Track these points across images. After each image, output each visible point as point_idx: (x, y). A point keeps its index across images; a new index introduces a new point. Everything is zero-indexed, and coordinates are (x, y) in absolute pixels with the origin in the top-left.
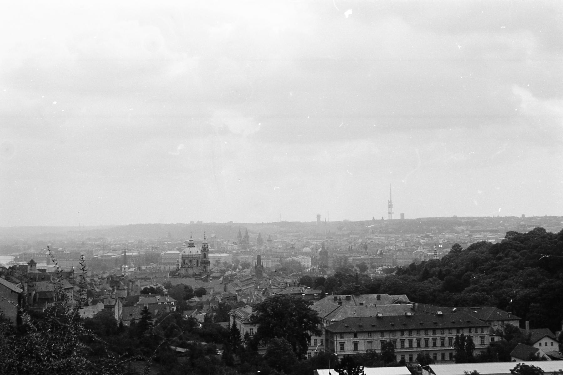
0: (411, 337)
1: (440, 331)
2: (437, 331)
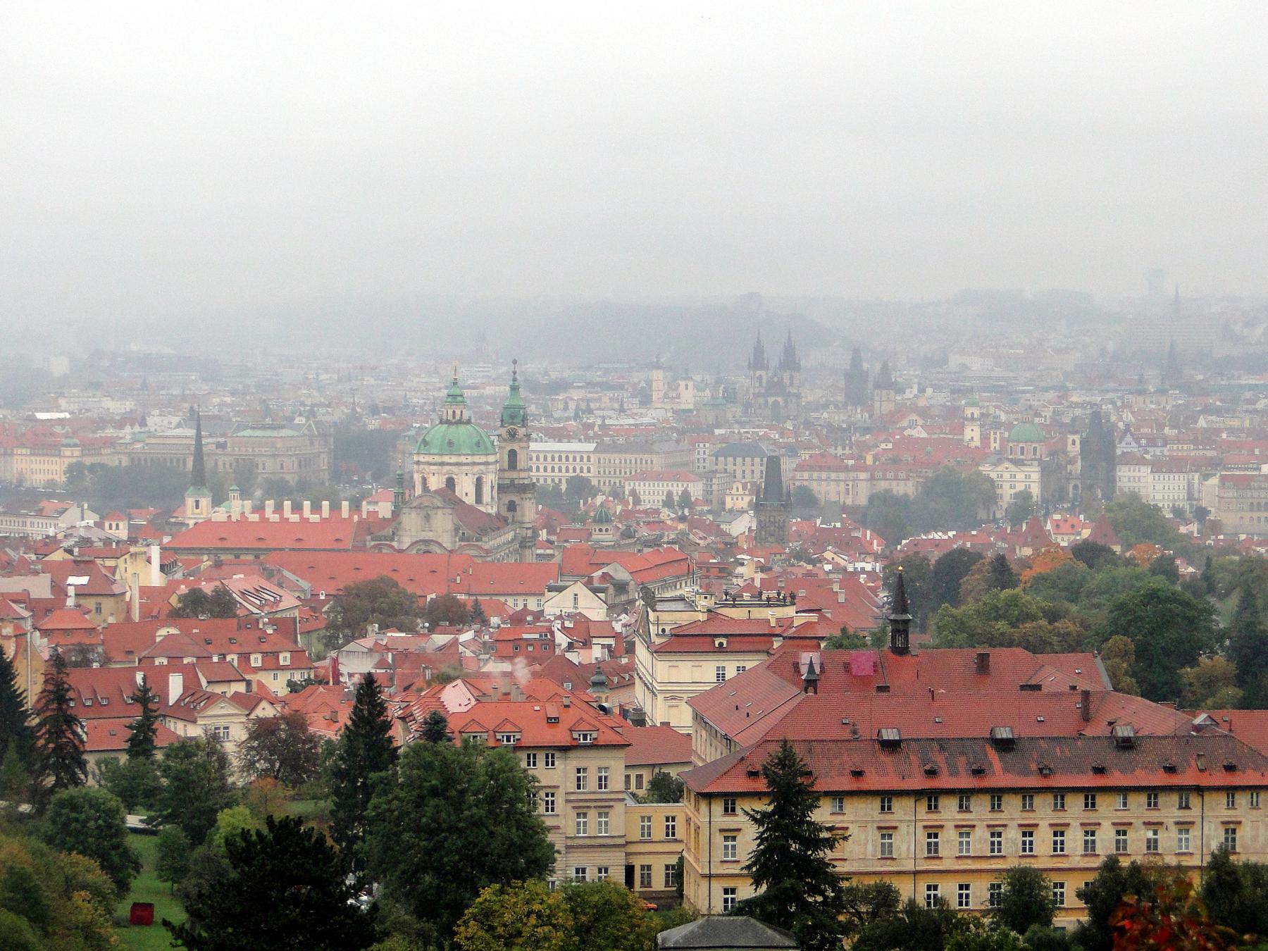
0: (998, 818)
1: (1175, 798)
2: (1038, 800)
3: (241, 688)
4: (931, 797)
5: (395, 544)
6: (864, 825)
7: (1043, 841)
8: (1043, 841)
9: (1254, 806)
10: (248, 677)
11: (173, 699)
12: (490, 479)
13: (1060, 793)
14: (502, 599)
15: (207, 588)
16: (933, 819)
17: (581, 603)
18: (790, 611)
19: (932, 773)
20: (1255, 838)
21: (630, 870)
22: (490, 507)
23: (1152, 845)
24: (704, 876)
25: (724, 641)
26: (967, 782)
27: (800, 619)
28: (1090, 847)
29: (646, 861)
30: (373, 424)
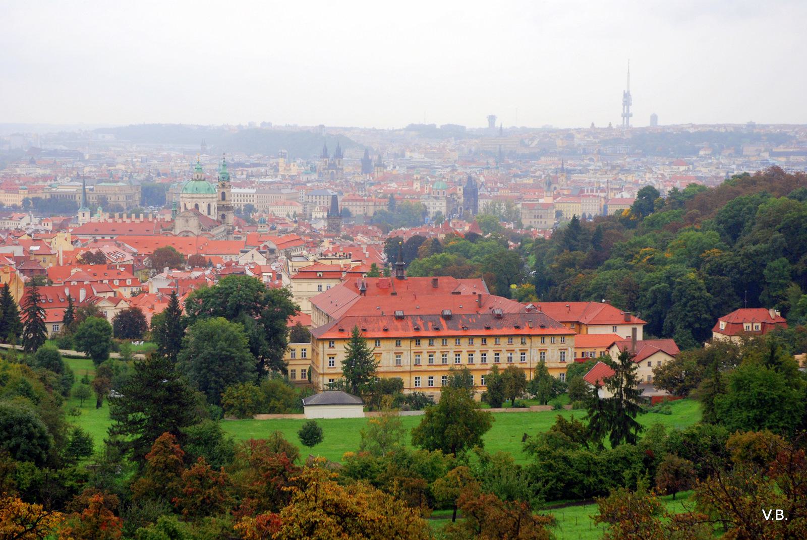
0: (445, 349)
3: (112, 294)
4: (417, 340)
5: (173, 232)
6: (388, 351)
7: (464, 359)
9: (553, 343)
10: (114, 290)
12: (214, 205)
13: (471, 338)
14: (221, 256)
15: (94, 252)
16: (418, 349)
17: (255, 258)
18: (349, 261)
19: (417, 329)
20: (553, 357)
22: (214, 216)
23: (510, 359)
24: (320, 374)
25: (321, 274)
26: (432, 333)
27: (354, 265)
28: (484, 360)
29: (293, 368)
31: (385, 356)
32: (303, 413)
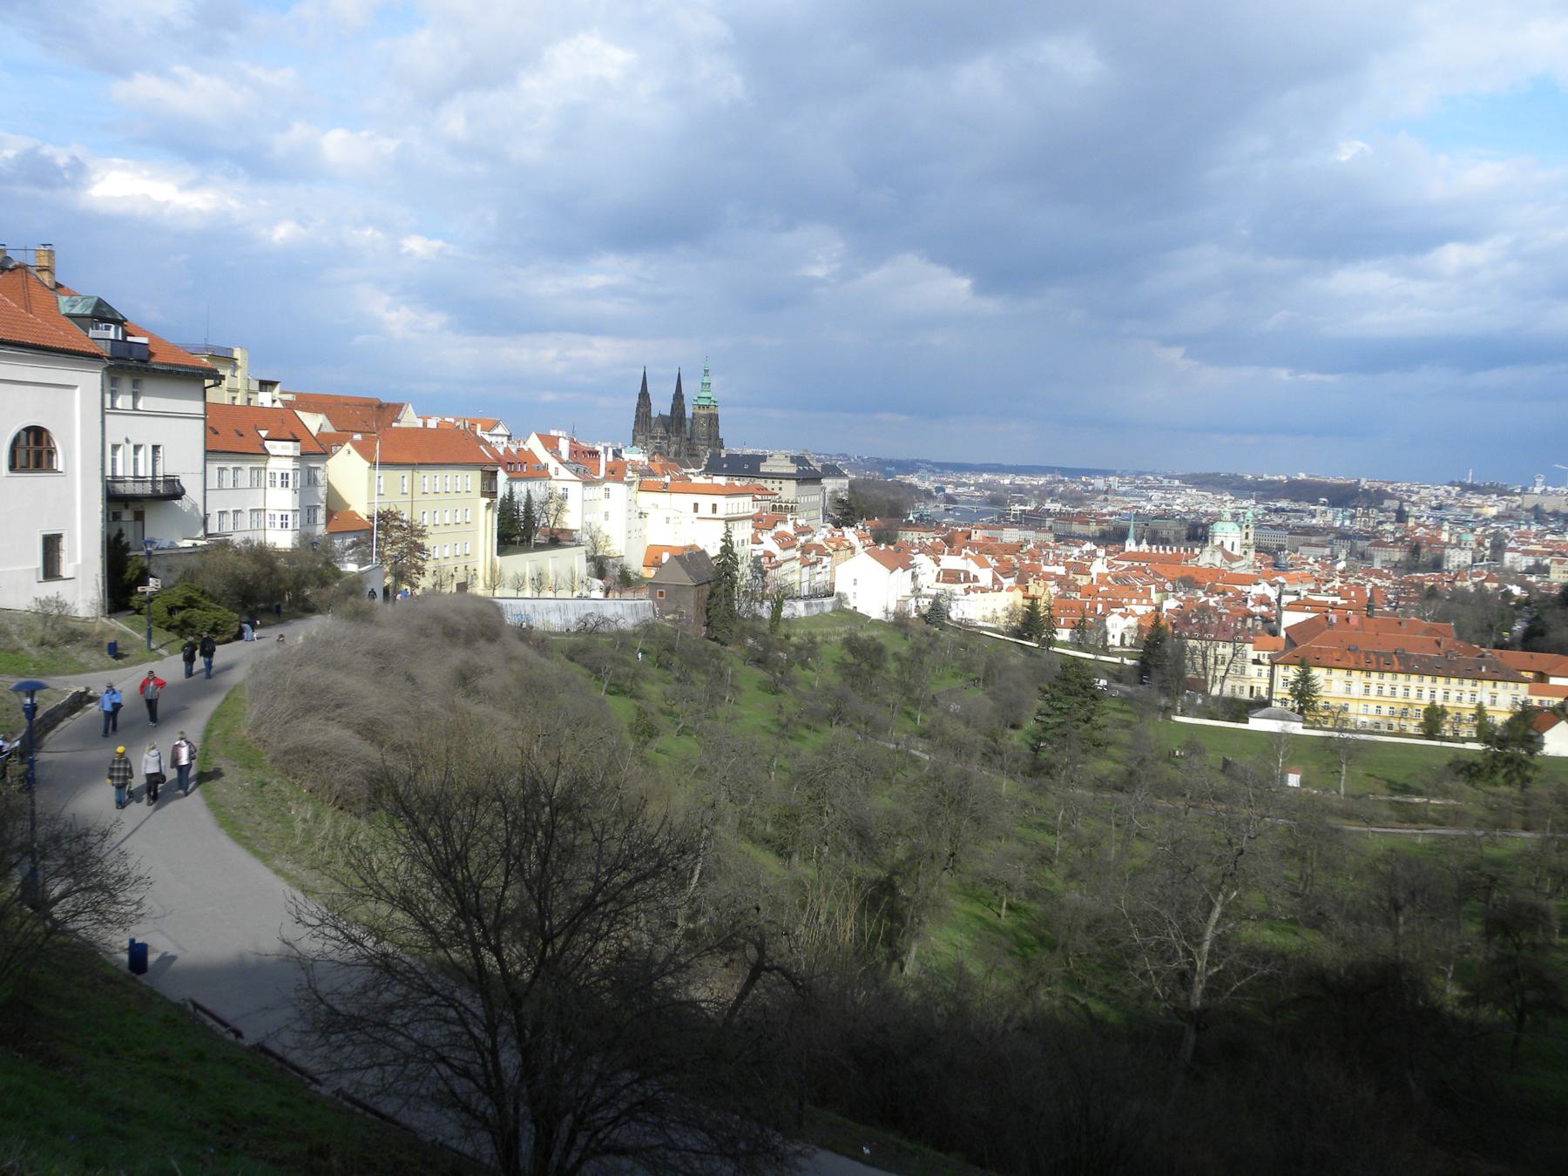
0: (1394, 682)
3: (1123, 610)
8: (1413, 693)
11: (1098, 612)
16: (1367, 680)
18: (1338, 600)
21: (1252, 688)
22: (1237, 552)
23: (1459, 699)
29: (1259, 685)
30: (1204, 521)
31: (1335, 683)
32: (1247, 723)
